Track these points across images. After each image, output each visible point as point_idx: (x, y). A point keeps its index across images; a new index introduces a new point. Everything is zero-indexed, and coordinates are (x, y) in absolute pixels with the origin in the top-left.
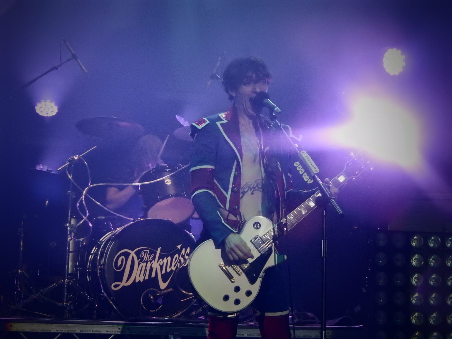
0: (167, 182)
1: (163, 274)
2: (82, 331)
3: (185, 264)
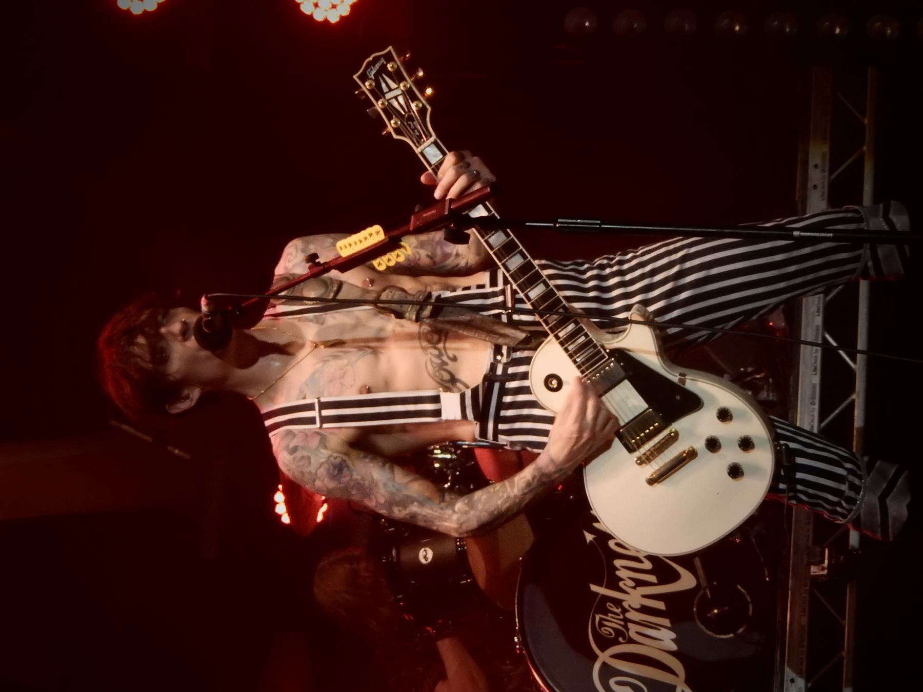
0: (425, 557)
1: (658, 579)
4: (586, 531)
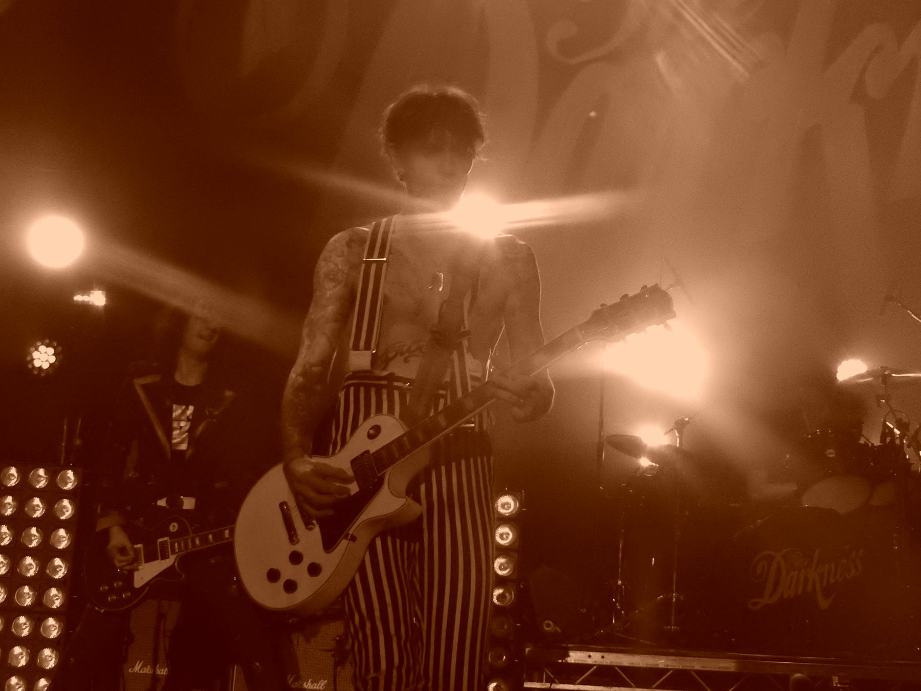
2: (703, 667)
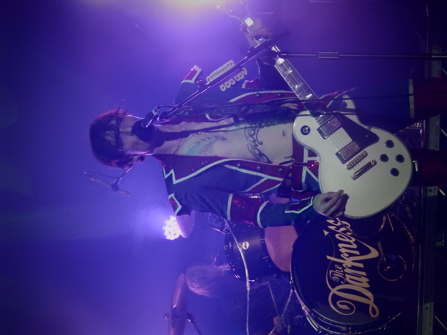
0: (245, 246)
3: (348, 226)
4: (325, 230)
